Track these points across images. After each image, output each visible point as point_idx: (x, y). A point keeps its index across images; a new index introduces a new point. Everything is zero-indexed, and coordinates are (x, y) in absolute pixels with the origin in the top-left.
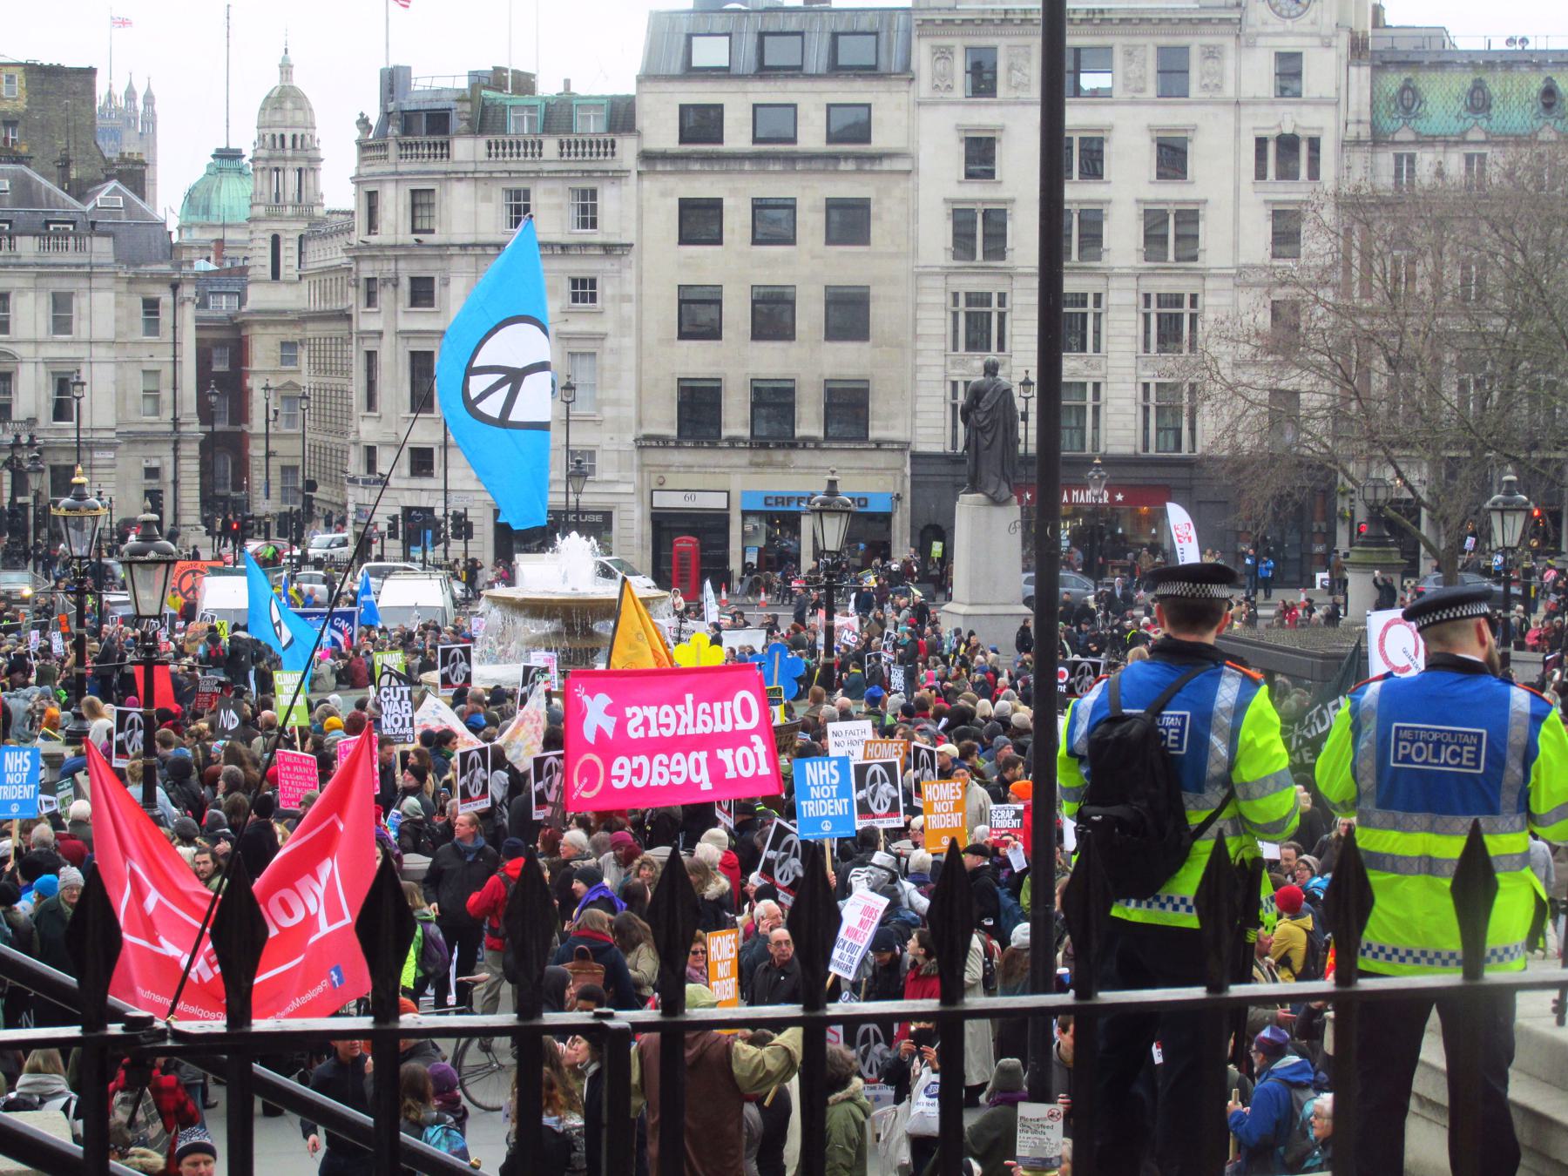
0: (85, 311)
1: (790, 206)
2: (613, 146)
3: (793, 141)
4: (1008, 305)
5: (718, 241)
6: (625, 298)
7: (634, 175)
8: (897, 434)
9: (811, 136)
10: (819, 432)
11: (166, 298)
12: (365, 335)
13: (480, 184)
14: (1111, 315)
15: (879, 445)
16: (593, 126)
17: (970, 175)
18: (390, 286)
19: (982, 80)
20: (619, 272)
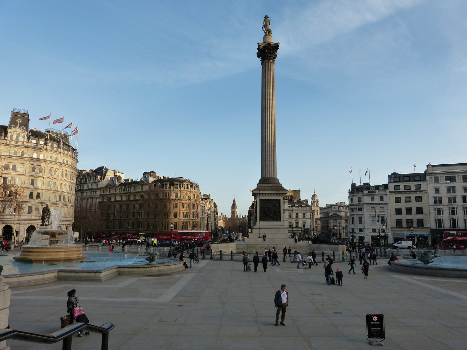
0: (306, 215)
1: (410, 198)
2: (385, 191)
3: (410, 189)
4: (443, 209)
5: (401, 202)
6: (388, 210)
7: (388, 194)
8: (428, 226)
9: (413, 189)
10: (417, 226)
11: (312, 214)
12: (351, 215)
13: (368, 196)
14: (459, 210)
15: (426, 228)
16: (381, 189)
17: (436, 193)
18: (356, 209)
19: (436, 180)
20: (387, 206)
